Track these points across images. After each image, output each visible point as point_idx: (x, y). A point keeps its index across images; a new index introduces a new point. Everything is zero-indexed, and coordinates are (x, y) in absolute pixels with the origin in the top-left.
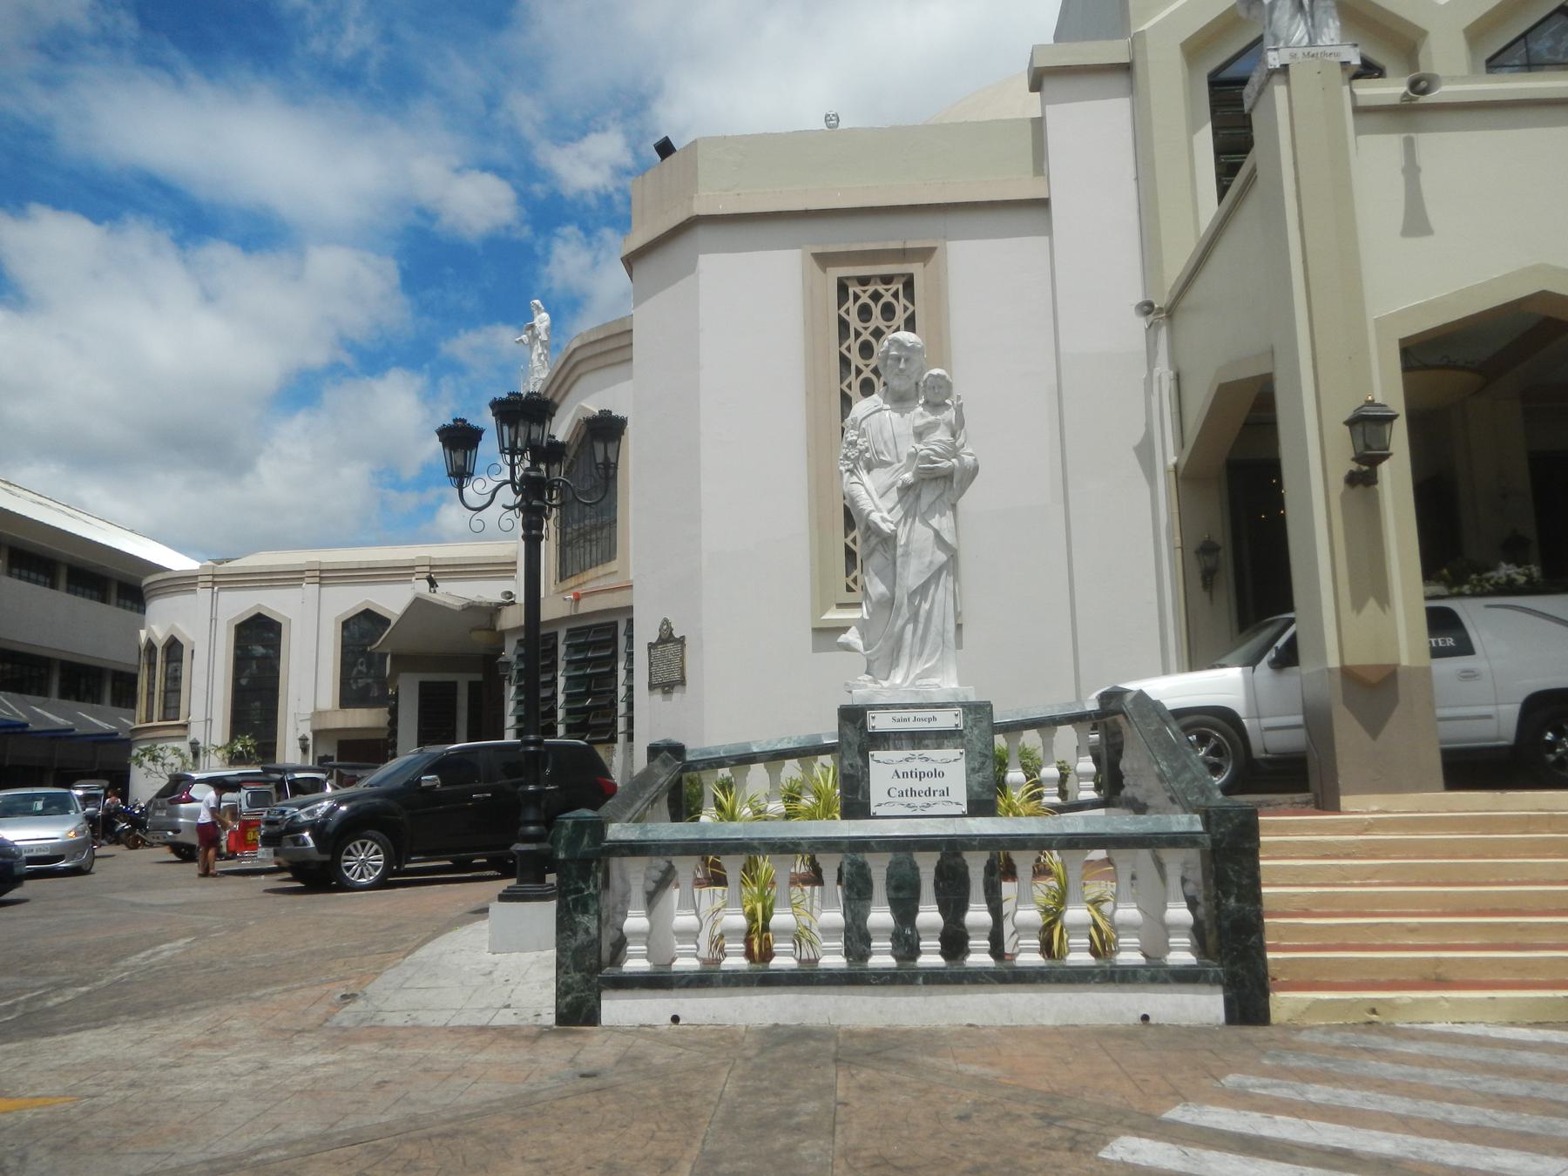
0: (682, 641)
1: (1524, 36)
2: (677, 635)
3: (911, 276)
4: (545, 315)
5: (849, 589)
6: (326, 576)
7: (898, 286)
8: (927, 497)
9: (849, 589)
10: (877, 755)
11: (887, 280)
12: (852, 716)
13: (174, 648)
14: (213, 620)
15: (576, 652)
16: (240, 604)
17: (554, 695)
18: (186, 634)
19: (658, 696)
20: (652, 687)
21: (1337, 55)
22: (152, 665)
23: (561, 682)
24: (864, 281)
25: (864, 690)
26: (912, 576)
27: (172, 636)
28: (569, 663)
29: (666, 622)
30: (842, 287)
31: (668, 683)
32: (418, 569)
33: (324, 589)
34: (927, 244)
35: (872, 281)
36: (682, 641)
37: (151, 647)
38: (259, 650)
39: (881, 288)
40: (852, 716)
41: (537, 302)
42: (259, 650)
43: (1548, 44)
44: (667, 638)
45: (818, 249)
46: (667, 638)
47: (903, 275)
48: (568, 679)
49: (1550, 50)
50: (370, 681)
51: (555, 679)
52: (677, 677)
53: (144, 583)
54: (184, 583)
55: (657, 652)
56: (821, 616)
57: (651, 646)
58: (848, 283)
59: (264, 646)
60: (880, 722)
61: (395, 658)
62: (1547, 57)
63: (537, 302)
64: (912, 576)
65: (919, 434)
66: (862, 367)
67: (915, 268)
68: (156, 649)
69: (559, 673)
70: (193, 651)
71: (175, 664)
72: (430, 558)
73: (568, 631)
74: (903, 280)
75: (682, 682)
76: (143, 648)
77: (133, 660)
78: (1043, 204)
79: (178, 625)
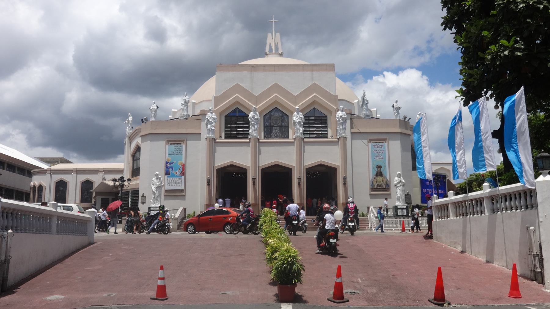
0: (145, 196)
1: (270, 112)
4: (131, 117)
6: (79, 172)
8: (158, 188)
10: (151, 212)
12: (149, 208)
13: (41, 187)
14: (51, 181)
15: (133, 195)
16: (57, 178)
17: (128, 203)
18: (44, 184)
19: (142, 204)
20: (141, 203)
22: (34, 191)
23: (130, 200)
25: (152, 205)
26: (156, 195)
27: (40, 184)
28: (131, 197)
29: (143, 194)
31: (143, 203)
32: (100, 171)
33: (78, 176)
34: (184, 139)
36: (145, 196)
37: (34, 187)
38: (62, 188)
40: (149, 208)
41: (129, 114)
42: (62, 188)
44: (143, 196)
45: (168, 139)
46: (143, 196)
48: (131, 200)
50: (88, 197)
51: (129, 200)
52: (144, 202)
53: (32, 171)
54: (43, 172)
55: (142, 198)
57: (141, 197)
59: (63, 188)
60: (152, 209)
61: (96, 193)
63: (129, 114)
64: (156, 195)
65: (158, 182)
68: (36, 187)
69: (130, 199)
70: (45, 188)
71: (40, 191)
72: (103, 168)
73: (132, 191)
75: (145, 202)
76: (32, 187)
77: (29, 190)
78: (201, 133)
79: (41, 182)
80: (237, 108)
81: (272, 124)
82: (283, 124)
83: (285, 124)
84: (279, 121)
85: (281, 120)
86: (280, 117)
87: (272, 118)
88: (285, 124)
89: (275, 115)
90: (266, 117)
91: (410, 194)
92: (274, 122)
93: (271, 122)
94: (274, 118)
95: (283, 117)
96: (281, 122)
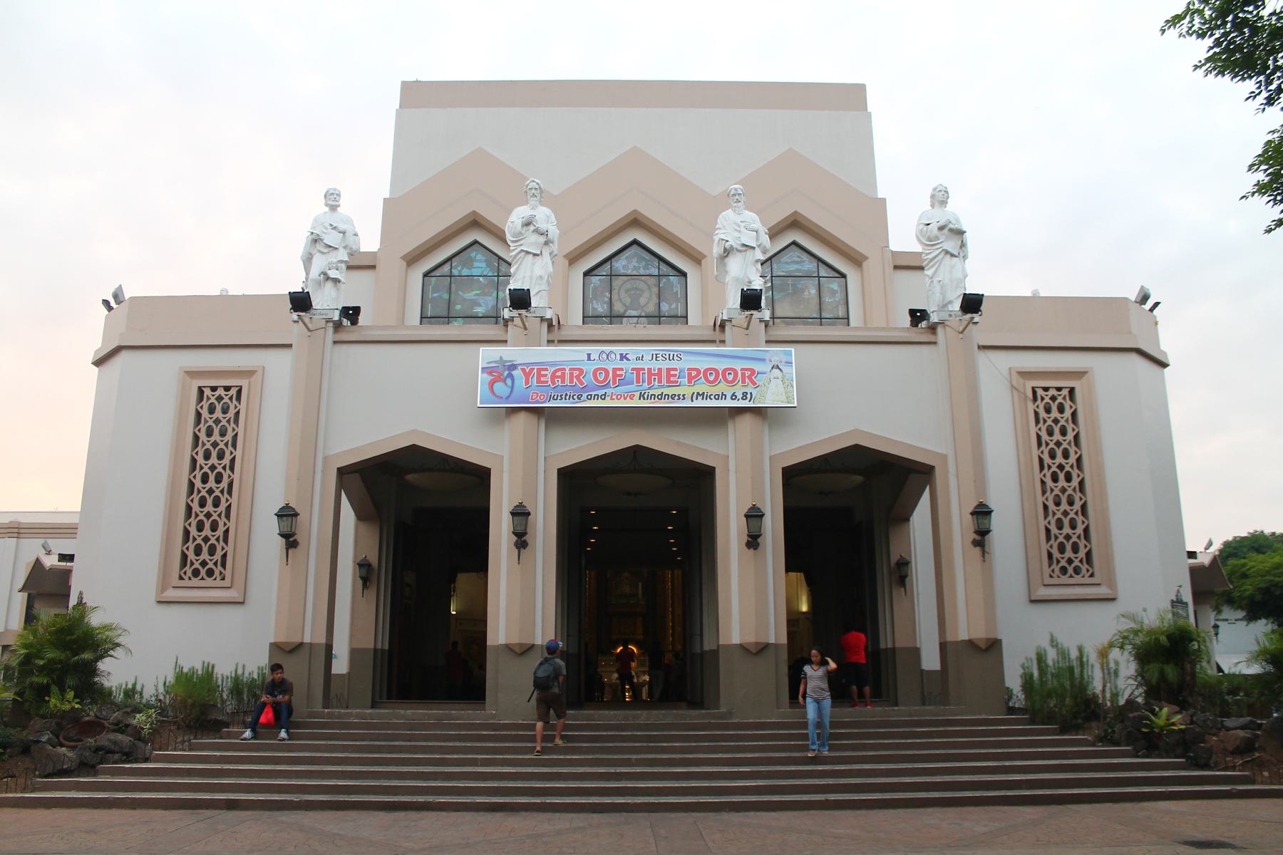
2: (84, 601)
3: (241, 387)
5: (181, 578)
7: (233, 392)
9: (181, 578)
11: (227, 389)
21: (326, 315)
24: (214, 389)
30: (201, 391)
35: (219, 389)
39: (221, 392)
43: (623, 264)
47: (237, 386)
49: (624, 267)
56: (162, 593)
58: (203, 389)
62: (622, 271)
66: (205, 442)
67: (244, 383)
74: (238, 388)
80: (476, 242)
81: (618, 308)
82: (662, 308)
83: (674, 306)
84: (646, 294)
85: (655, 290)
86: (653, 281)
87: (617, 282)
88: (674, 306)
89: (629, 272)
90: (595, 280)
91: (1185, 600)
92: (628, 301)
93: (615, 297)
94: (628, 286)
95: (664, 280)
96: (655, 300)
